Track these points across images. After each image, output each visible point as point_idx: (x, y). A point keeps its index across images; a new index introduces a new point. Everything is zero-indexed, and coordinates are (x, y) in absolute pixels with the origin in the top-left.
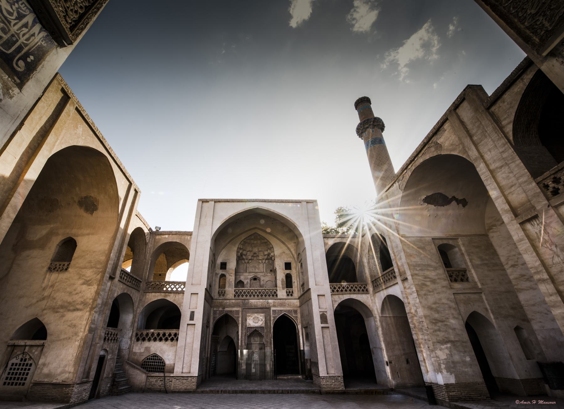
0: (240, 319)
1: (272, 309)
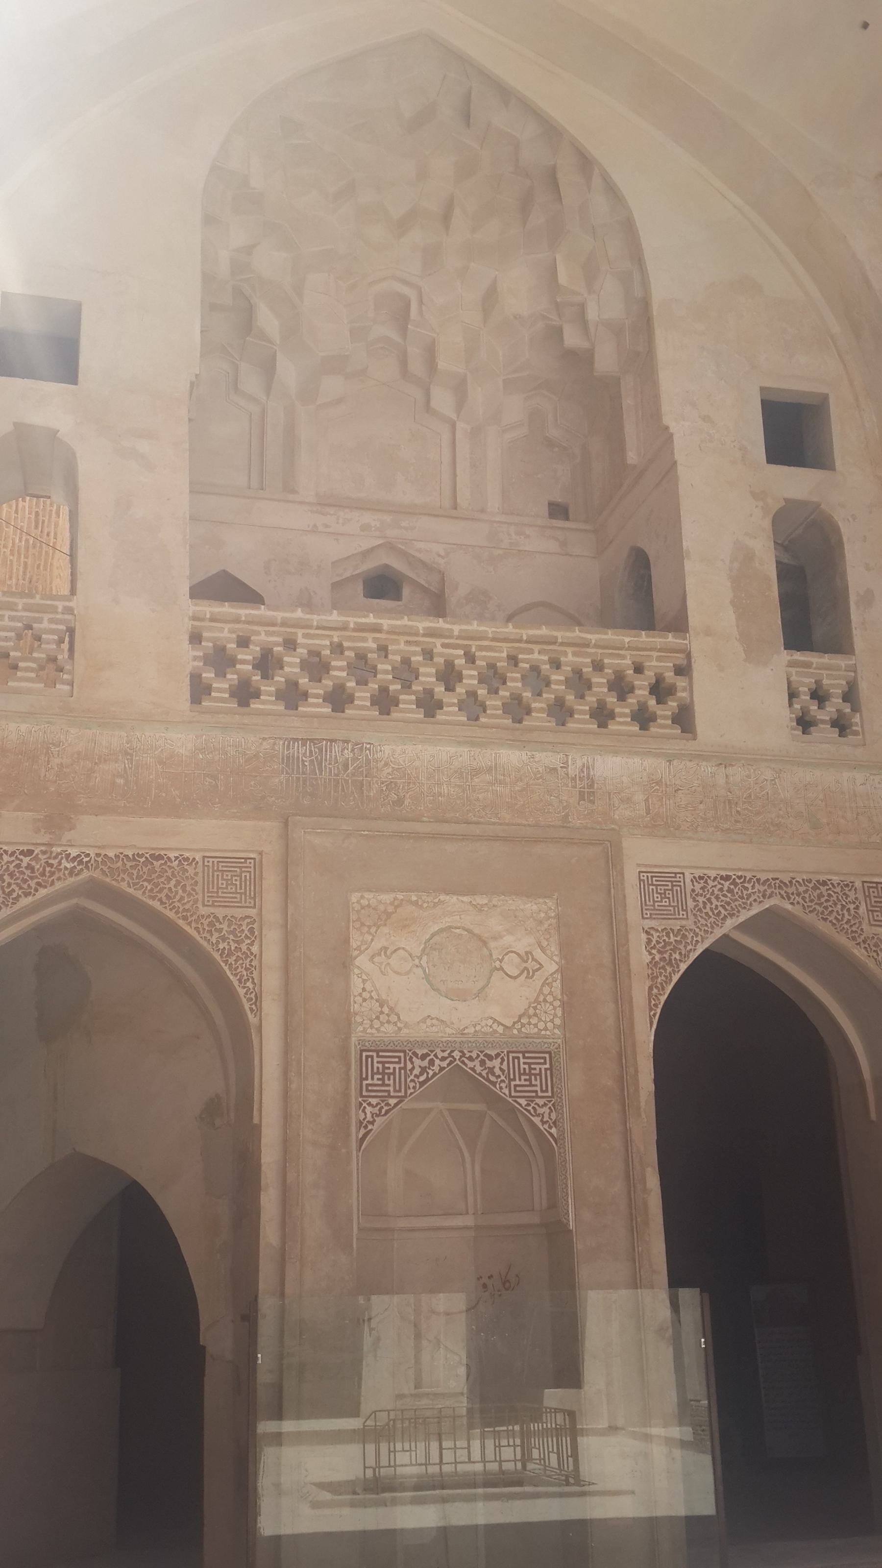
0: (272, 939)
1: (642, 853)
